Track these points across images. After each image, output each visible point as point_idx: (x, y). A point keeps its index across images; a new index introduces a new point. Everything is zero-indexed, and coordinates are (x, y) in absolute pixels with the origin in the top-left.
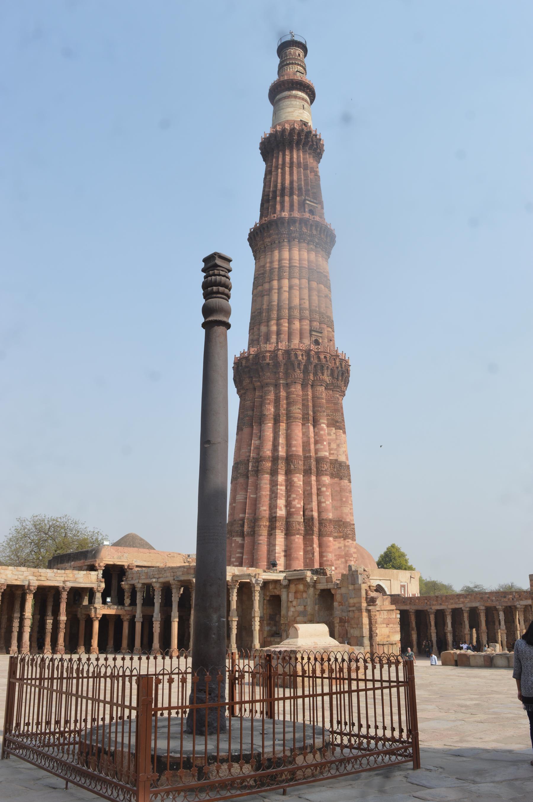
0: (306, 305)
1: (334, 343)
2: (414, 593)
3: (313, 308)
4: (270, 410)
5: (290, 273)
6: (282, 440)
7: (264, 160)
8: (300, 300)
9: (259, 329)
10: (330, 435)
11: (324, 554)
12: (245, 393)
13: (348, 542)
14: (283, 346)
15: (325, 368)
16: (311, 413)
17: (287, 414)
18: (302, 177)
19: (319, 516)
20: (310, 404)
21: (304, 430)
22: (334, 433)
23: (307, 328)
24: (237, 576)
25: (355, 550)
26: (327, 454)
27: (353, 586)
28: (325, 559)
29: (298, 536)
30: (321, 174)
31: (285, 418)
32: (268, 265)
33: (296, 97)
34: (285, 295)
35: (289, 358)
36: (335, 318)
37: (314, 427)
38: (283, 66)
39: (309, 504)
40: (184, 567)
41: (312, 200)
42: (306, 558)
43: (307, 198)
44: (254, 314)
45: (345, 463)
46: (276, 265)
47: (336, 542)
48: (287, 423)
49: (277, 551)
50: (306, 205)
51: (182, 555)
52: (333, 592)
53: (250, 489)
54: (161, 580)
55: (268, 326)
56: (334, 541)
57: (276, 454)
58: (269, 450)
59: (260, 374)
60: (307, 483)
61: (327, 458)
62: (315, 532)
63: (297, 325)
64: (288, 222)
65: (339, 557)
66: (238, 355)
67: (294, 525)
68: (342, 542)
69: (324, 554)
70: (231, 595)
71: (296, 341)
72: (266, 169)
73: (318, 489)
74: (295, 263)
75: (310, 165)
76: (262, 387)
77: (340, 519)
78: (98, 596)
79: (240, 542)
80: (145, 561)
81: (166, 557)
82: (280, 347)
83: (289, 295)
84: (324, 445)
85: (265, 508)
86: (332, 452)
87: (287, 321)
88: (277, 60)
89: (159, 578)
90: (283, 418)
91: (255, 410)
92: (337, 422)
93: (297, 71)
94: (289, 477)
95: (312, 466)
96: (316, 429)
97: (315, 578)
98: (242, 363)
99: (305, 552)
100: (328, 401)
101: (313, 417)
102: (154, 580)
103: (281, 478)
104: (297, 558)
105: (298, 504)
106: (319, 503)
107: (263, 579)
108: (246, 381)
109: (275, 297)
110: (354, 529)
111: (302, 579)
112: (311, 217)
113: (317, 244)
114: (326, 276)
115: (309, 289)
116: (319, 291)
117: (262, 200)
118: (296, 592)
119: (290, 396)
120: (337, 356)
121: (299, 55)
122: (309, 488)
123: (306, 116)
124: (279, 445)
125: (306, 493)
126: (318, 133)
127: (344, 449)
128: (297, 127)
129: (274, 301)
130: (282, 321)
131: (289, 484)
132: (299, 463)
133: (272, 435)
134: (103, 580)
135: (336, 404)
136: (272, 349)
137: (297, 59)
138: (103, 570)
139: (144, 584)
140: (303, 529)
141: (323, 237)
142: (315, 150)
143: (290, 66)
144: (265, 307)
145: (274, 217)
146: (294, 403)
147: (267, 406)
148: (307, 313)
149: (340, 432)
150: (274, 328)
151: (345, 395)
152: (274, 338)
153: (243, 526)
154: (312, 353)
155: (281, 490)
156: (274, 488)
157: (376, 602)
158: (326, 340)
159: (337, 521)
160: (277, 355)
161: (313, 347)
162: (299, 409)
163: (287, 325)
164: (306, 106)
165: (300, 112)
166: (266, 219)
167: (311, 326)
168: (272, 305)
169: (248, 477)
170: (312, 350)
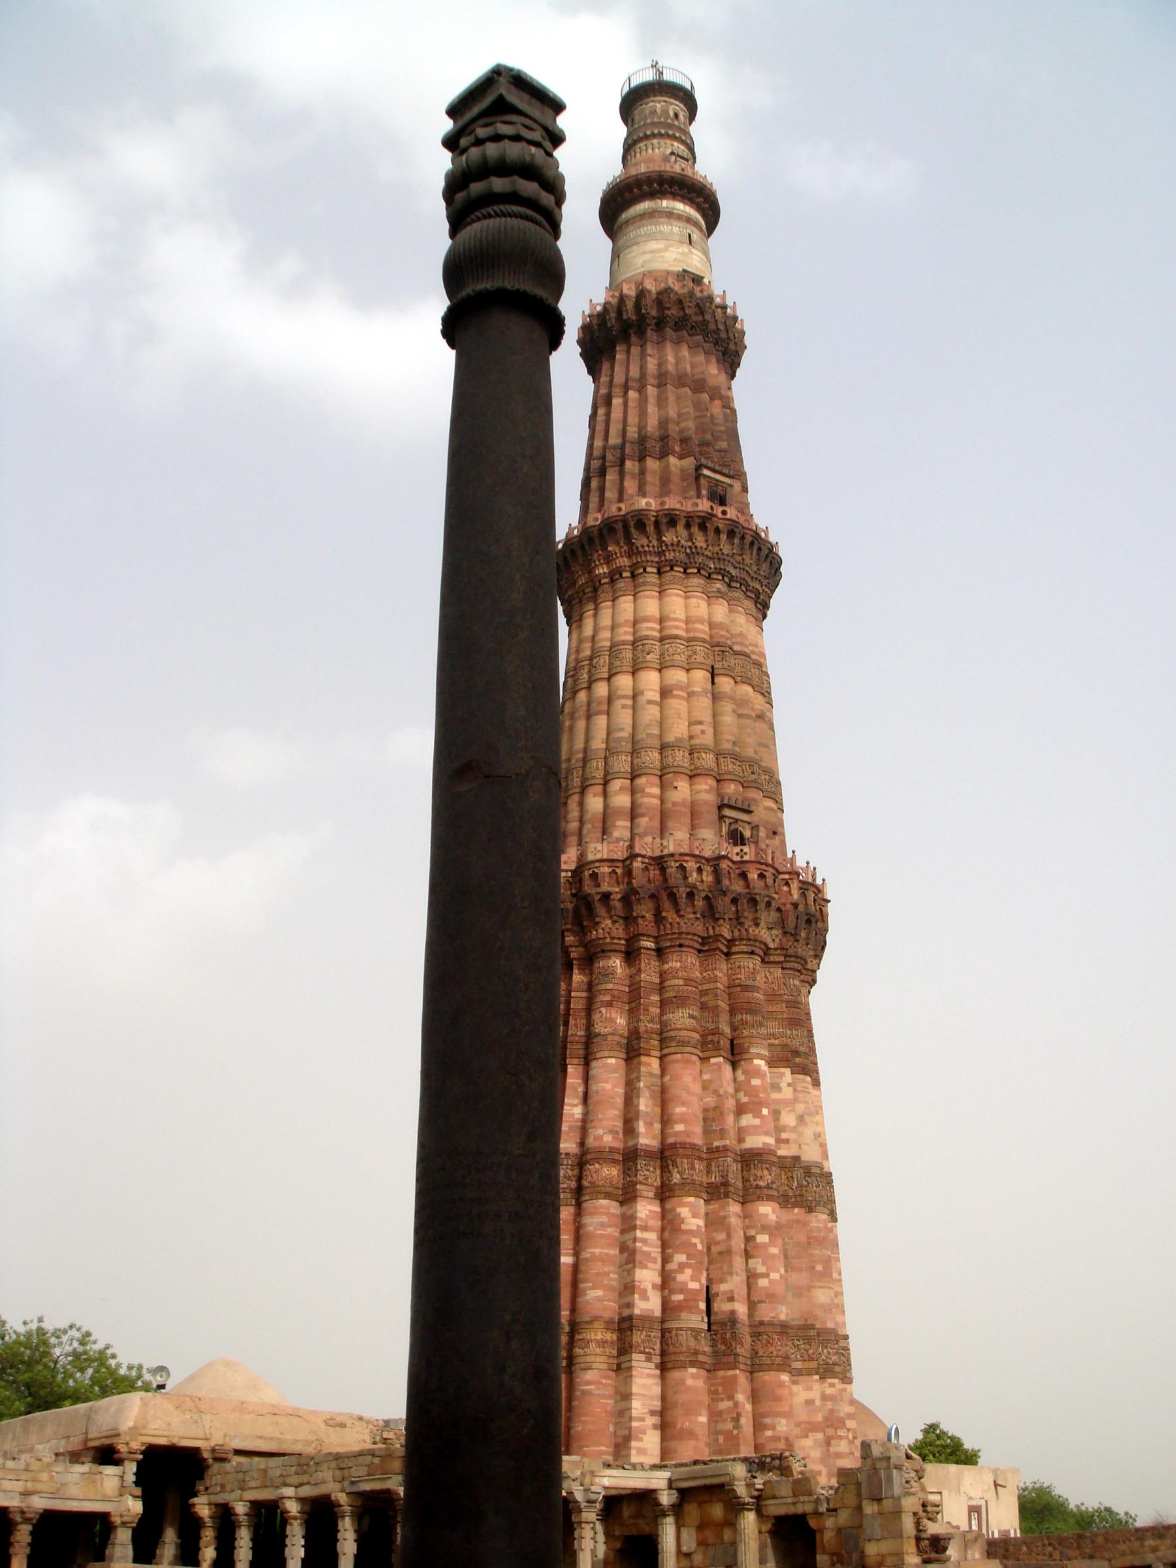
0: (708, 739)
1: (783, 842)
2: (1004, 1527)
3: (726, 746)
4: (613, 1021)
5: (662, 655)
6: (645, 1104)
7: (589, 373)
8: (690, 724)
9: (581, 804)
10: (779, 1089)
11: (768, 1420)
14: (648, 846)
18: (691, 410)
19: (751, 1315)
20: (723, 1005)
21: (706, 1077)
22: (789, 1085)
23: (711, 798)
25: (851, 1409)
26: (771, 1141)
27: (875, 1503)
28: (769, 1433)
29: (694, 1370)
30: (738, 404)
31: (656, 1043)
32: (606, 634)
33: (670, 215)
34: (651, 713)
36: (785, 775)
37: (734, 1065)
38: (635, 143)
41: (717, 468)
42: (717, 1433)
45: (822, 1168)
48: (661, 1058)
49: (634, 1413)
50: (703, 481)
51: (368, 1422)
52: (813, 1523)
54: (306, 1491)
55: (605, 794)
56: (795, 1383)
57: (630, 1143)
58: (611, 1132)
59: (585, 923)
60: (714, 1222)
61: (772, 1153)
63: (682, 790)
64: (657, 524)
65: (810, 1428)
67: (683, 1339)
69: (768, 1420)
72: (596, 392)
73: (748, 1239)
74: (677, 628)
75: (712, 382)
76: (589, 960)
78: (123, 1537)
81: (323, 1426)
82: (637, 850)
83: (661, 712)
84: (762, 1117)
85: (600, 1293)
86: (784, 1136)
87: (657, 780)
88: (622, 131)
89: (301, 1485)
91: (572, 1022)
92: (796, 1053)
93: (672, 153)
94: (668, 1206)
95: (731, 1175)
96: (739, 1072)
97: (759, 1483)
99: (715, 1416)
100: (772, 997)
101: (732, 1041)
102: (289, 1491)
103: (646, 1209)
104: (691, 1434)
105: (691, 1281)
106: (751, 1277)
107: (605, 1488)
109: (624, 718)
110: (847, 1349)
111: (721, 1486)
112: (718, 510)
113: (732, 578)
114: (759, 665)
115: (713, 695)
116: (742, 702)
117: (587, 469)
118: (700, 1528)
119: (667, 983)
121: (676, 116)
123: (694, 262)
124: (637, 1118)
125: (715, 1249)
126: (729, 303)
127: (818, 1129)
129: (622, 729)
130: (641, 781)
131: (669, 1226)
132: (693, 1168)
133: (621, 1091)
134: (138, 1491)
136: (620, 854)
137: (671, 126)
139: (256, 1505)
140: (707, 1349)
141: (748, 561)
143: (655, 141)
144: (598, 744)
145: (620, 509)
148: (708, 760)
151: (814, 981)
152: (621, 829)
154: (724, 865)
155: (645, 1241)
156: (627, 1236)
157: (945, 1549)
159: (799, 1328)
160: (629, 873)
161: (727, 849)
162: (691, 1017)
163: (656, 791)
165: (680, 250)
166: (599, 516)
167: (720, 795)
168: (615, 740)
170: (725, 857)
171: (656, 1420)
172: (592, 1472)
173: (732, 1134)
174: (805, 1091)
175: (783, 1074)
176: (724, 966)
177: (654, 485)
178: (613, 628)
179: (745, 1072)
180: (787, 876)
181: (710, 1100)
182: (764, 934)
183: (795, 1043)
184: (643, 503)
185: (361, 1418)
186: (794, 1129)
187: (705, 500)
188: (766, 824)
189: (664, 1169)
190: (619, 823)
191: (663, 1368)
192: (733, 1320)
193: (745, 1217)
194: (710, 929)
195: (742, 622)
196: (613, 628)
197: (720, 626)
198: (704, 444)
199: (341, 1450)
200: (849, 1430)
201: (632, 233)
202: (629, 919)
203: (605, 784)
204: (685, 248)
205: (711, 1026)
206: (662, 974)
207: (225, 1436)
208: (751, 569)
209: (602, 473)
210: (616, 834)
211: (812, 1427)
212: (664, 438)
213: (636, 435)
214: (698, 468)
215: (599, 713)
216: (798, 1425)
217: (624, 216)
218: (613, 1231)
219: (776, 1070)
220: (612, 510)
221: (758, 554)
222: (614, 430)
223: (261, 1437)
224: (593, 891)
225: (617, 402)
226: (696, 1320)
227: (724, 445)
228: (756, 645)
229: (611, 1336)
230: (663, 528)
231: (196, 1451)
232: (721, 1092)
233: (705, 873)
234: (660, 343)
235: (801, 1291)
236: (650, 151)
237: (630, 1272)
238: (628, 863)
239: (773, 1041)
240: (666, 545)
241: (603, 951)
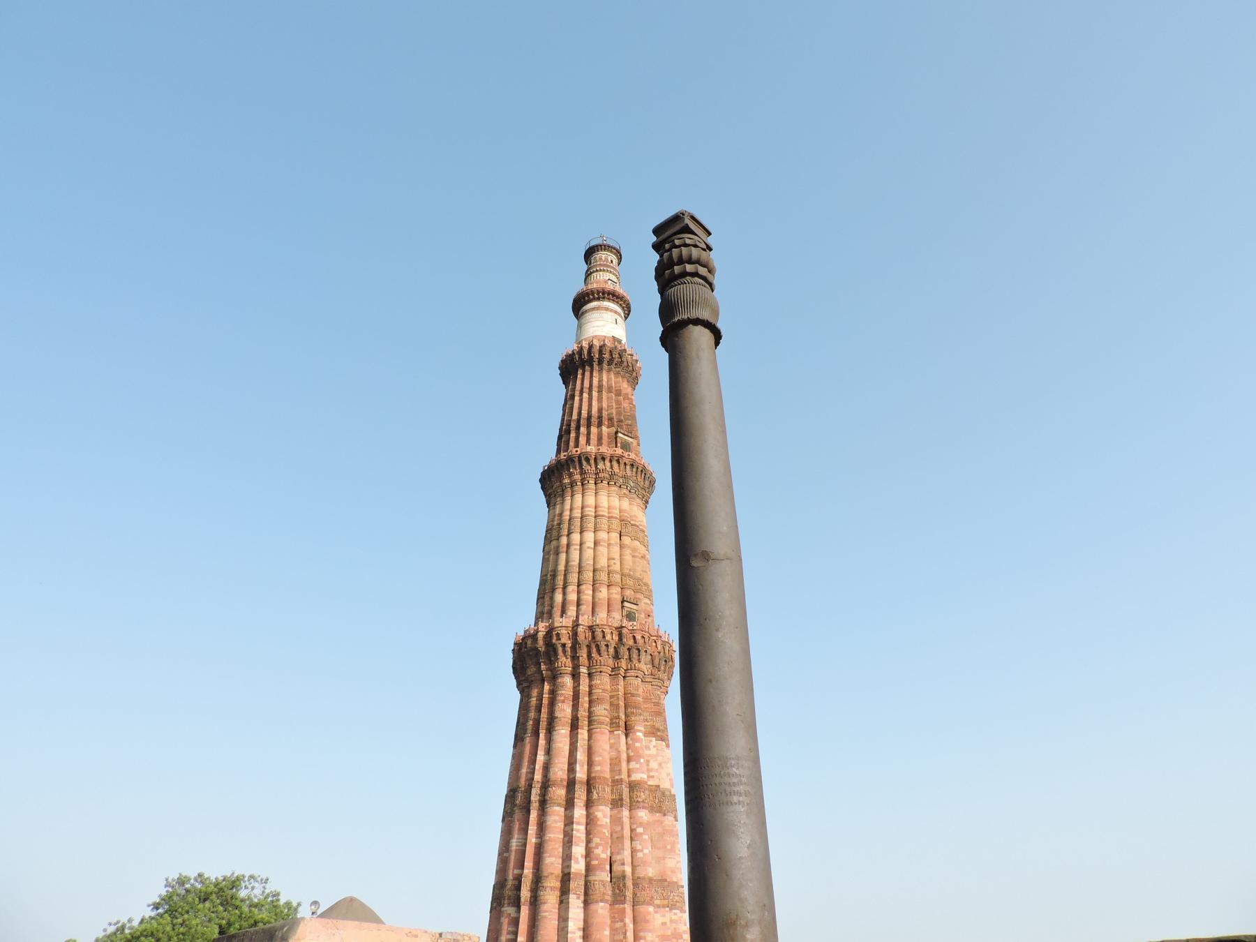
0: (617, 567)
3: (626, 571)
4: (564, 711)
6: (581, 756)
9: (552, 598)
11: (642, 934)
12: (528, 687)
14: (585, 620)
15: (643, 653)
17: (589, 717)
20: (622, 704)
23: (619, 597)
26: (645, 776)
32: (567, 513)
33: (607, 309)
34: (589, 553)
35: (594, 637)
36: (652, 587)
37: (627, 735)
39: (618, 853)
47: (657, 916)
48: (589, 731)
53: (532, 829)
55: (564, 594)
60: (616, 821)
63: (603, 593)
64: (595, 459)
66: (521, 633)
68: (668, 915)
69: (642, 934)
71: (602, 616)
73: (632, 830)
75: (624, 391)
79: (514, 915)
88: (586, 267)
90: (584, 723)
99: (614, 931)
100: (646, 700)
103: (579, 812)
105: (602, 853)
106: (634, 851)
108: (531, 670)
109: (575, 555)
112: (626, 454)
116: (634, 550)
117: (561, 429)
122: (618, 828)
128: (609, 344)
130: (583, 587)
131: (590, 821)
133: (567, 748)
135: (657, 704)
144: (561, 567)
146: (600, 701)
148: (617, 578)
150: (572, 597)
152: (572, 611)
153: (518, 888)
154: (625, 631)
155: (578, 831)
160: (575, 634)
161: (625, 623)
164: (619, 320)
169: (528, 812)
171: (581, 933)
174: (662, 750)
176: (621, 682)
178: (571, 510)
181: (614, 754)
182: (643, 666)
183: (658, 725)
184: (589, 448)
188: (645, 611)
189: (589, 792)
191: (586, 903)
197: (625, 511)
201: (588, 316)
202: (575, 658)
203: (565, 587)
206: (590, 686)
209: (568, 432)
212: (600, 417)
214: (616, 433)
218: (561, 825)
220: (573, 451)
225: (577, 398)
226: (605, 876)
229: (558, 884)
235: (660, 860)
237: (570, 847)
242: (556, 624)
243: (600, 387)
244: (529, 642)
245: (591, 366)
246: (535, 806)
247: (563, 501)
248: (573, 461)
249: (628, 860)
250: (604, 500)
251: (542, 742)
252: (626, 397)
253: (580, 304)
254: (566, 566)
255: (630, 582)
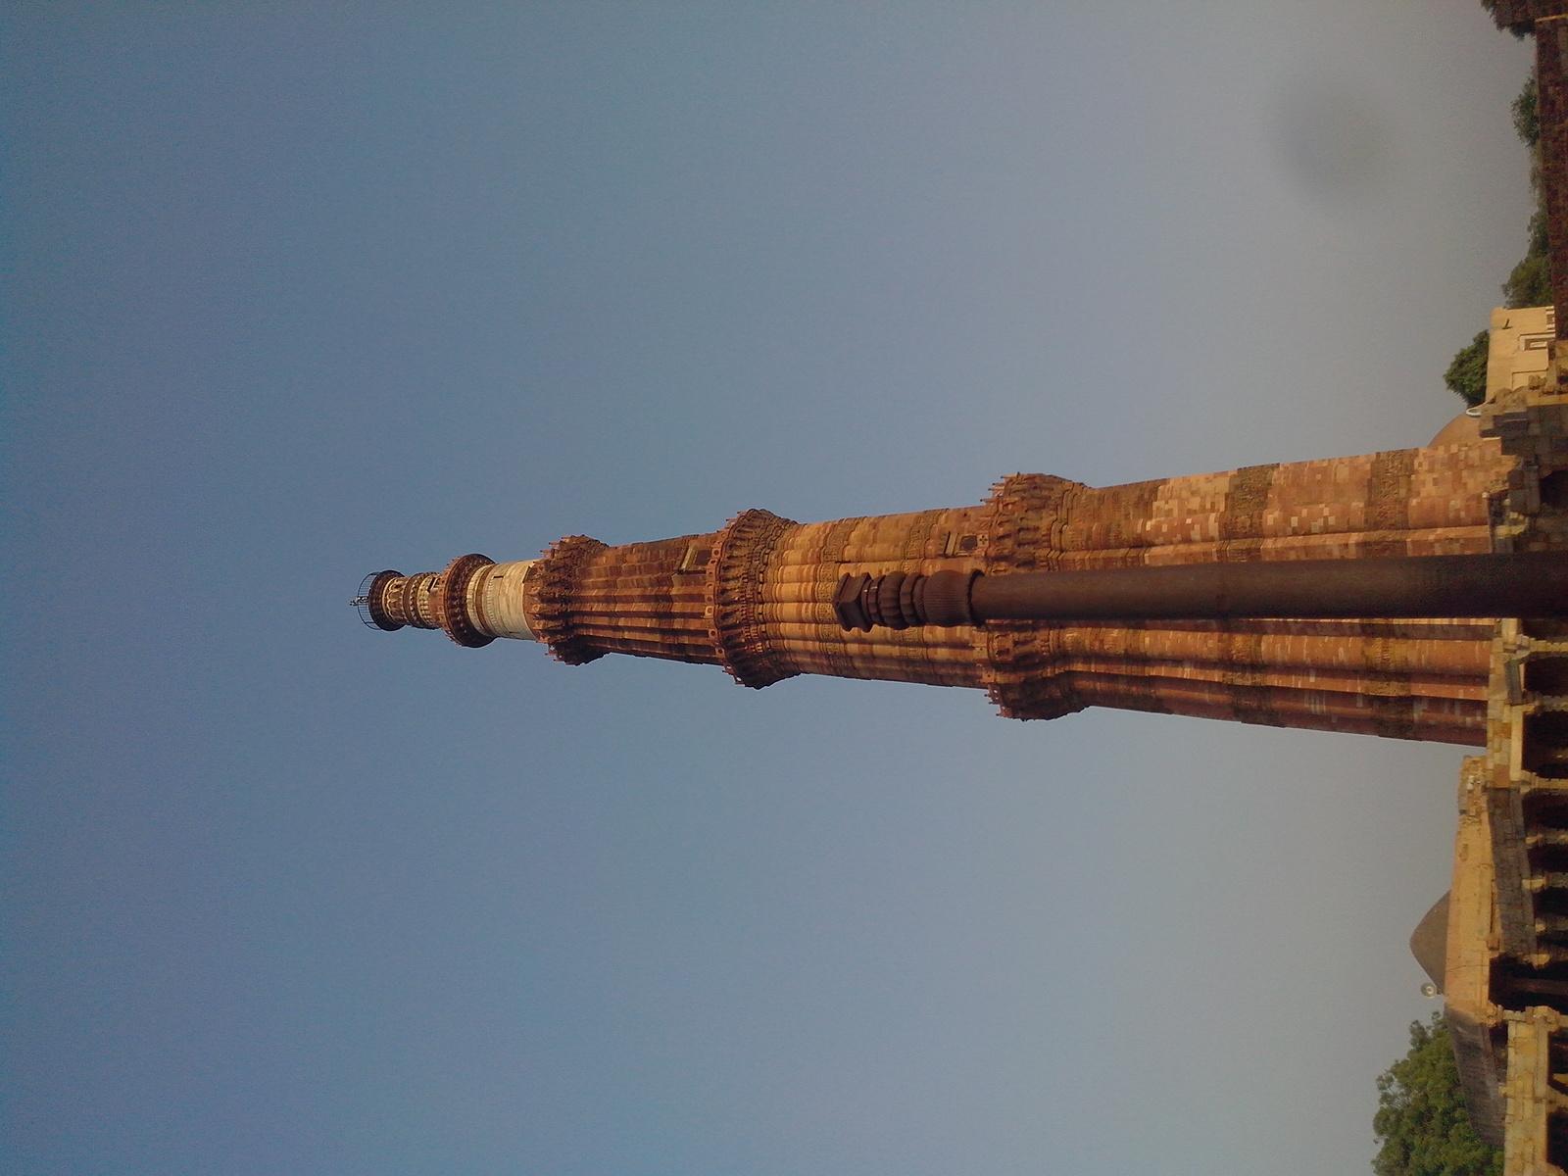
3: (898, 553)
10: (1171, 510)
11: (1451, 515)
12: (1079, 693)
13: (1420, 465)
15: (1024, 523)
16: (1122, 552)
19: (1360, 530)
20: (1103, 554)
22: (1167, 503)
24: (1511, 693)
26: (1213, 517)
27: (1532, 425)
28: (1463, 514)
33: (479, 592)
37: (1151, 545)
38: (419, 619)
39: (1330, 553)
40: (1492, 816)
41: (681, 557)
43: (675, 568)
44: (911, 676)
46: (810, 629)
52: (1546, 473)
53: (1297, 682)
54: (1526, 872)
55: (936, 645)
56: (1418, 494)
59: (1037, 661)
62: (1398, 538)
65: (1458, 480)
68: (1422, 478)
70: (1558, 710)
73: (1295, 533)
74: (806, 589)
77: (1366, 484)
79: (1424, 706)
80: (1479, 911)
84: (1193, 524)
85: (1341, 650)
86: (1208, 506)
93: (428, 590)
96: (1157, 541)
97: (1514, 515)
98: (1013, 701)
100: (1096, 516)
101: (1133, 547)
102: (1526, 884)
106: (1326, 530)
107: (1518, 633)
110: (1388, 454)
116: (864, 540)
120: (998, 500)
121: (397, 587)
123: (516, 572)
129: (885, 632)
135: (1101, 499)
138: (1506, 1008)
142: (581, 552)
144: (895, 651)
145: (713, 633)
147: (1106, 647)
149: (1163, 492)
151: (1082, 484)
153: (1384, 700)
154: (992, 552)
158: (966, 525)
159: (1370, 491)
161: (979, 552)
166: (717, 650)
167: (938, 556)
168: (893, 638)
169: (1270, 688)
170: (986, 553)
172: (1505, 643)
173: (1205, 547)
175: (1158, 508)
176: (1070, 555)
177: (693, 606)
178: (805, 639)
179: (1158, 538)
180: (1001, 505)
182: (1044, 524)
185: (1459, 833)
186: (1203, 498)
187: (707, 567)
190: (958, 634)
192: (1363, 545)
193: (1276, 536)
194: (1042, 564)
195: (802, 539)
196: (805, 639)
197: (804, 556)
198: (661, 567)
199: (1488, 844)
200: (1459, 450)
201: (492, 619)
203: (926, 645)
204: (506, 581)
205: (1119, 564)
207: (1478, 939)
208: (759, 530)
209: (682, 647)
210: (966, 637)
211: (1458, 480)
212: (657, 598)
213: (654, 620)
214: (680, 572)
215: (872, 651)
216: (1455, 491)
217: (478, 629)
219: (1154, 514)
221: (749, 527)
222: (649, 637)
223: (1479, 911)
224: (1012, 654)
225: (627, 635)
227: (662, 552)
228: (819, 529)
229: (1379, 641)
230: (728, 600)
231: (1494, 964)
232: (1172, 555)
233: (999, 568)
234: (583, 600)
236: (426, 607)
238: (990, 628)
239: (1131, 516)
240: (742, 597)
241: (1059, 647)
242: (985, 656)
243: (608, 600)
244: (1011, 696)
245: (573, 614)
246: (1259, 679)
247: (790, 651)
248: (729, 639)
249: (1339, 538)
250: (789, 589)
251: (1162, 671)
252: (622, 558)
253: (472, 635)
254: (892, 643)
255: (914, 547)
